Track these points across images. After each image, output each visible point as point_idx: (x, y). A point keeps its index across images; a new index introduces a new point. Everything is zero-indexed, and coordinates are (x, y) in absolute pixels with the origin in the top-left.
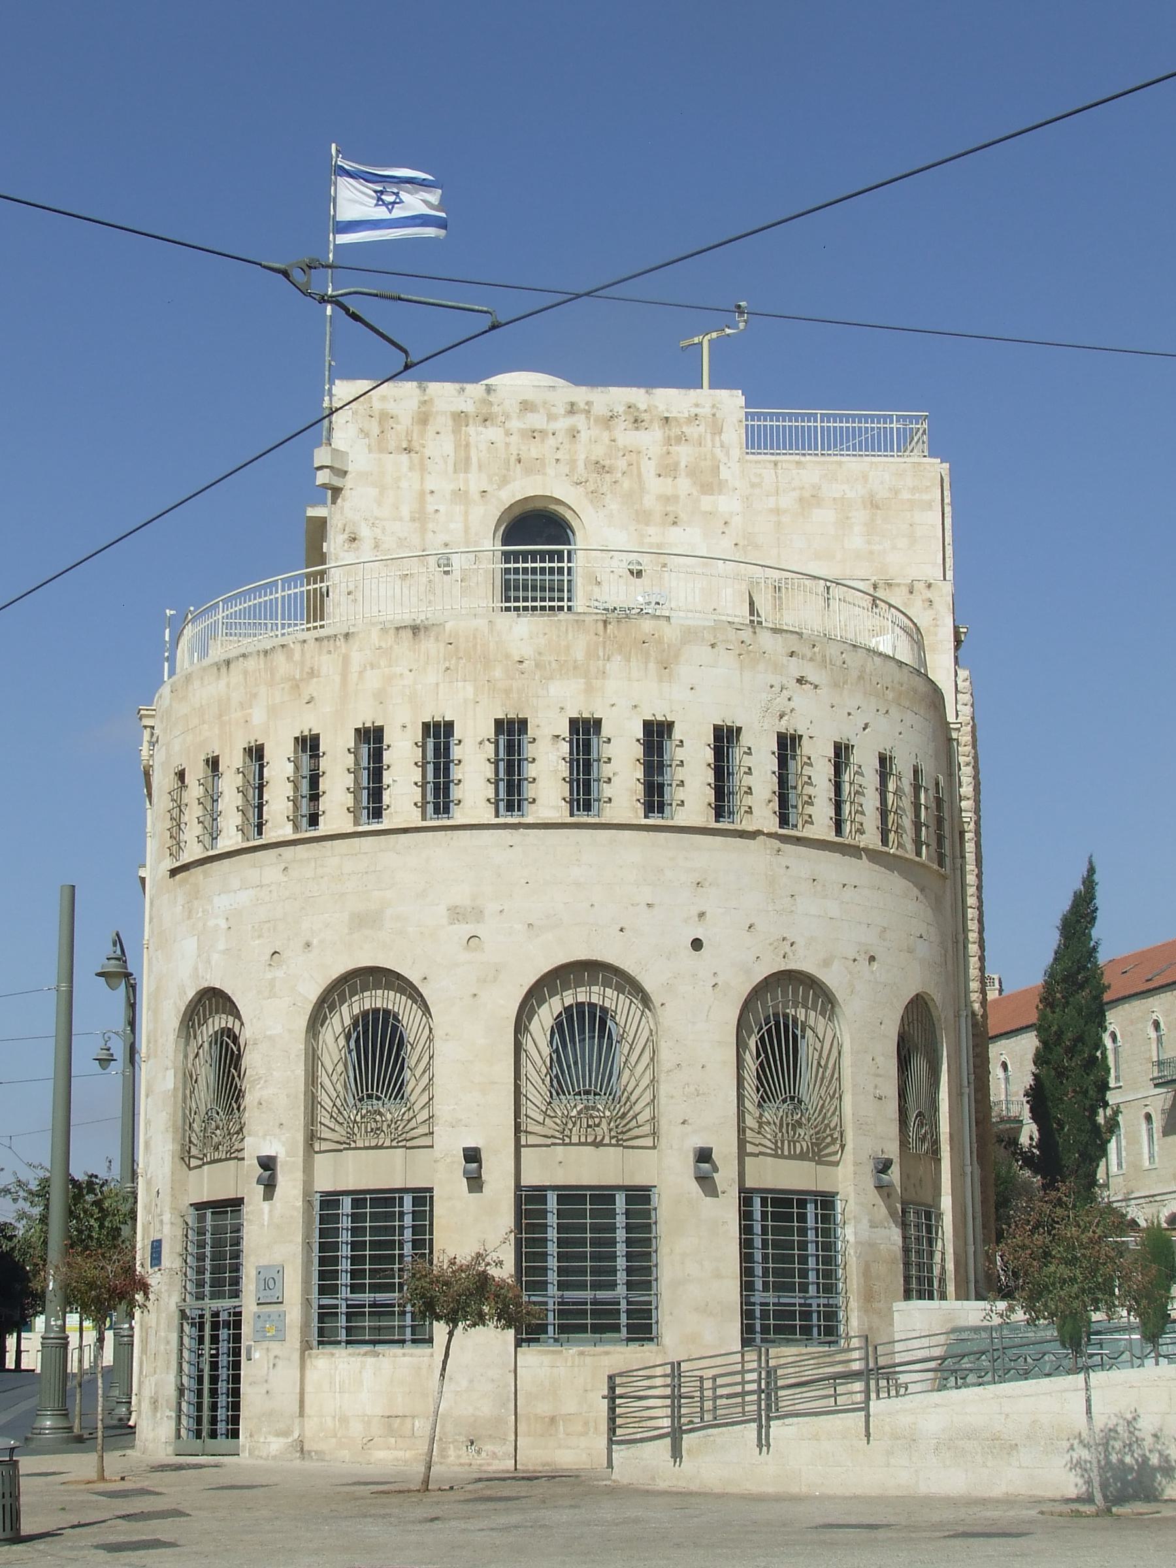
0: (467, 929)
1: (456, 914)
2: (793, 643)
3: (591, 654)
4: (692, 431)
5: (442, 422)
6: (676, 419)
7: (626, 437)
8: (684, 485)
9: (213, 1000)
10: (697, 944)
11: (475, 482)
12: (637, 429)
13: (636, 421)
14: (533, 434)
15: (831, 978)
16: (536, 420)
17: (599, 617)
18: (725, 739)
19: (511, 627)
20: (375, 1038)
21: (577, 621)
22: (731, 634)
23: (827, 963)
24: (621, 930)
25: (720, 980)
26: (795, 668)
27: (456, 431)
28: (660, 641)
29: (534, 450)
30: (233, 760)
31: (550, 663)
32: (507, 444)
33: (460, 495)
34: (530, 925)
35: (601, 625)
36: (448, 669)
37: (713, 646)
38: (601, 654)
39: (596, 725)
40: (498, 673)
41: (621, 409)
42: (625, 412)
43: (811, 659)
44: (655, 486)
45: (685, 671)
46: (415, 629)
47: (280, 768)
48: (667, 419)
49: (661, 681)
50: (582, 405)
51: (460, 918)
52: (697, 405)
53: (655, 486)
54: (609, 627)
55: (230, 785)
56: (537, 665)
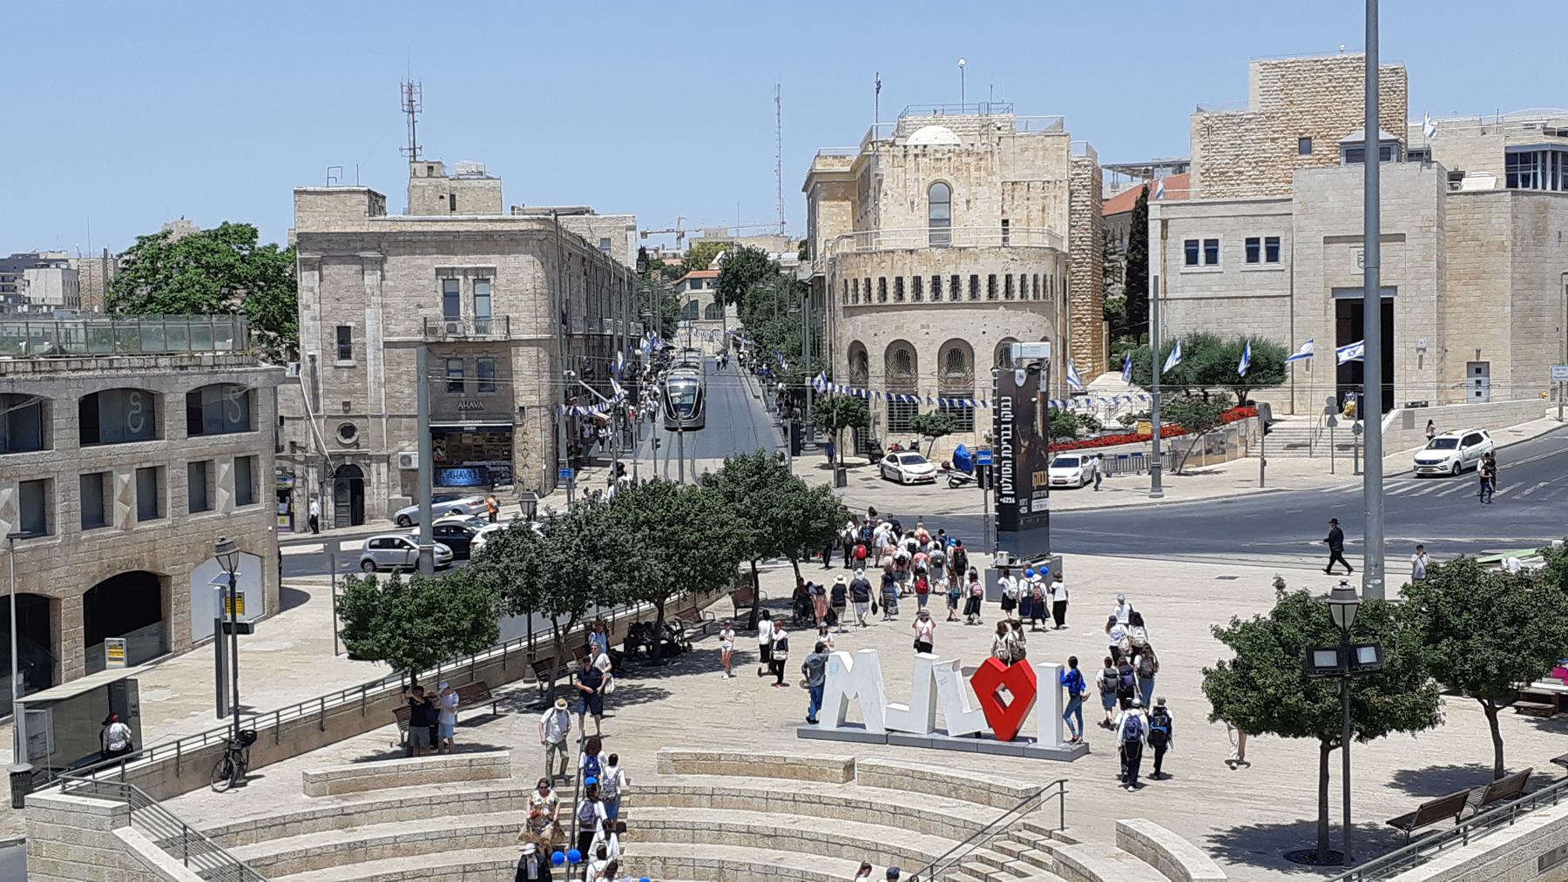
1: (923, 327)
5: (911, 157)
7: (965, 159)
8: (983, 173)
9: (856, 342)
11: (921, 175)
14: (937, 159)
16: (939, 155)
18: (992, 278)
20: (902, 355)
29: (938, 165)
30: (862, 282)
33: (917, 180)
44: (974, 174)
46: (911, 252)
47: (875, 285)
53: (974, 174)
55: (861, 288)
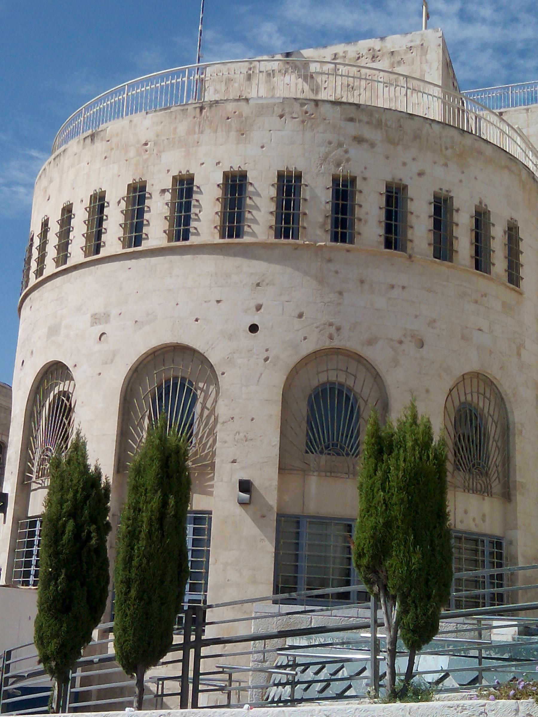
0: (99, 329)
1: (96, 319)
2: (352, 112)
3: (190, 132)
4: (409, 57)
6: (398, 52)
10: (254, 328)
12: (374, 61)
13: (373, 57)
15: (377, 355)
17: (198, 105)
19: (142, 122)
21: (183, 110)
22: (297, 107)
23: (371, 342)
24: (197, 320)
25: (271, 354)
26: (351, 129)
27: (268, 81)
28: (241, 115)
31: (163, 141)
32: (296, 84)
34: (136, 322)
35: (198, 110)
36: (105, 158)
37: (281, 116)
38: (197, 129)
39: (190, 179)
40: (132, 153)
41: (364, 52)
42: (367, 54)
43: (368, 123)
45: (257, 135)
48: (392, 53)
49: (238, 143)
50: (341, 54)
51: (97, 321)
52: (411, 41)
54: (204, 111)
56: (155, 144)
